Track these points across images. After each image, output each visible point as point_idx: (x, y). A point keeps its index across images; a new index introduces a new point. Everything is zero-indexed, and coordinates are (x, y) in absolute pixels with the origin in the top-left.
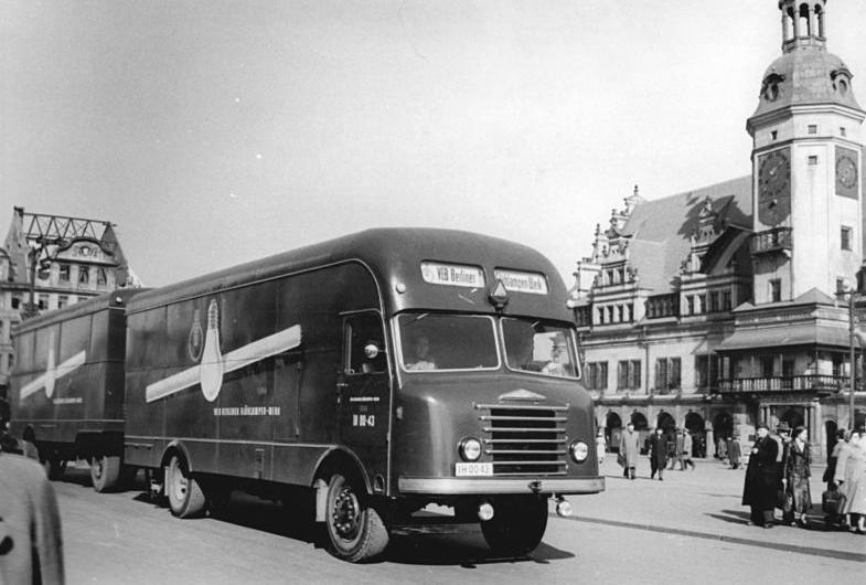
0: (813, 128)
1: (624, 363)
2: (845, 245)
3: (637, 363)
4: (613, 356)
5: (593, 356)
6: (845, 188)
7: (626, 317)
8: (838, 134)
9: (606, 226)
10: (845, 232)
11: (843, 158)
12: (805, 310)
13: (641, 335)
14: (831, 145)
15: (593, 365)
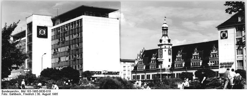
0: (165, 47)
1: (142, 75)
2: (170, 61)
3: (144, 75)
4: (140, 75)
5: (138, 74)
6: (169, 54)
7: (142, 69)
8: (168, 47)
9: (139, 54)
10: (170, 60)
11: (169, 50)
12: (164, 70)
13: (145, 72)
14: (168, 49)
15: (137, 76)
